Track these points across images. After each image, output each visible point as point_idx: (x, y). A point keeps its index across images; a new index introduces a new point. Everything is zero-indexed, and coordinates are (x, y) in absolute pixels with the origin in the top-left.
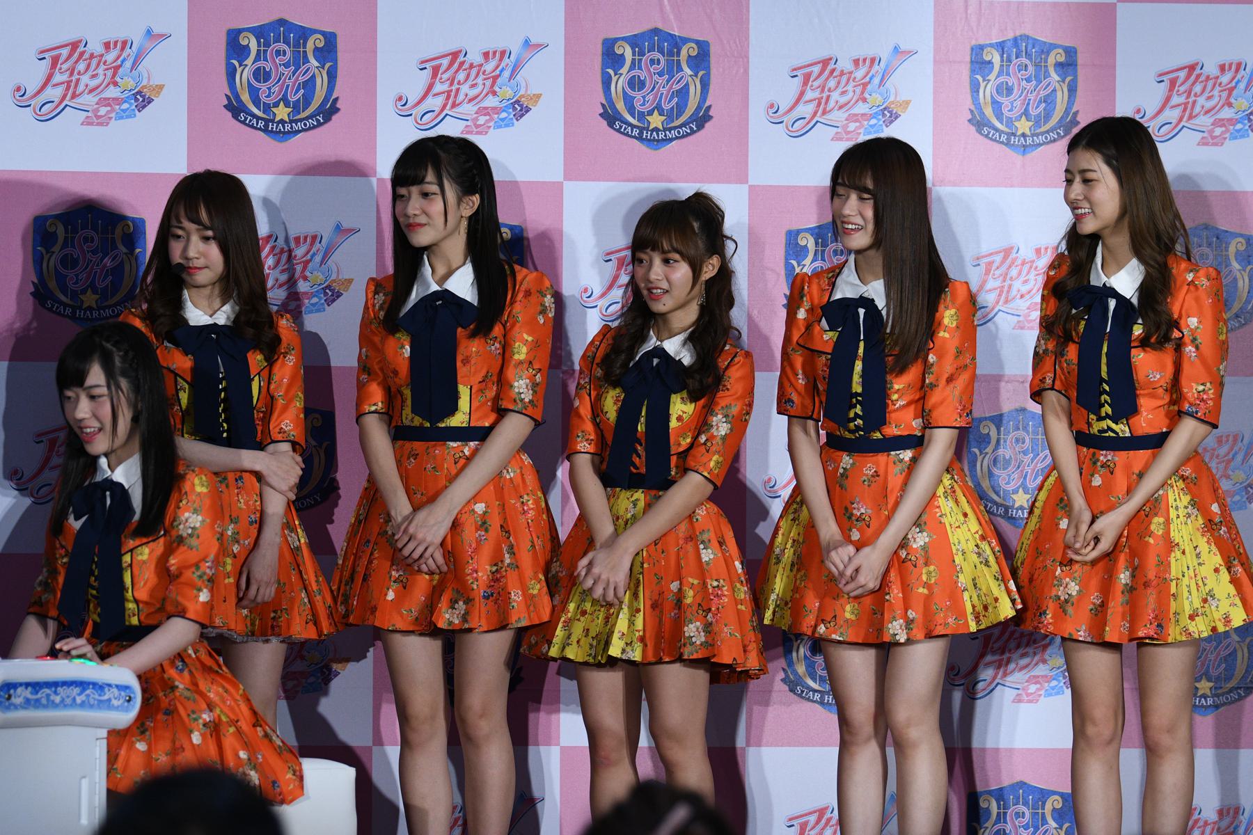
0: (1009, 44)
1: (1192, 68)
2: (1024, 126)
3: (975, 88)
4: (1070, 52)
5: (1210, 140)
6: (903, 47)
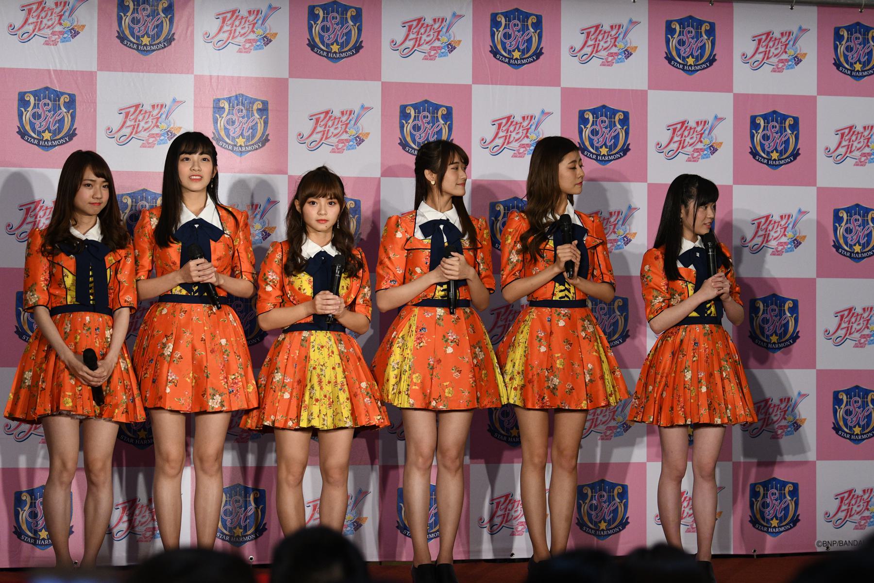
0: (233, 98)
1: (327, 113)
2: (241, 141)
3: (215, 121)
4: (265, 103)
5: (336, 150)
6: (178, 99)
